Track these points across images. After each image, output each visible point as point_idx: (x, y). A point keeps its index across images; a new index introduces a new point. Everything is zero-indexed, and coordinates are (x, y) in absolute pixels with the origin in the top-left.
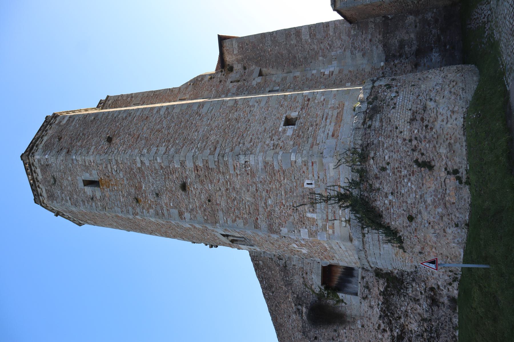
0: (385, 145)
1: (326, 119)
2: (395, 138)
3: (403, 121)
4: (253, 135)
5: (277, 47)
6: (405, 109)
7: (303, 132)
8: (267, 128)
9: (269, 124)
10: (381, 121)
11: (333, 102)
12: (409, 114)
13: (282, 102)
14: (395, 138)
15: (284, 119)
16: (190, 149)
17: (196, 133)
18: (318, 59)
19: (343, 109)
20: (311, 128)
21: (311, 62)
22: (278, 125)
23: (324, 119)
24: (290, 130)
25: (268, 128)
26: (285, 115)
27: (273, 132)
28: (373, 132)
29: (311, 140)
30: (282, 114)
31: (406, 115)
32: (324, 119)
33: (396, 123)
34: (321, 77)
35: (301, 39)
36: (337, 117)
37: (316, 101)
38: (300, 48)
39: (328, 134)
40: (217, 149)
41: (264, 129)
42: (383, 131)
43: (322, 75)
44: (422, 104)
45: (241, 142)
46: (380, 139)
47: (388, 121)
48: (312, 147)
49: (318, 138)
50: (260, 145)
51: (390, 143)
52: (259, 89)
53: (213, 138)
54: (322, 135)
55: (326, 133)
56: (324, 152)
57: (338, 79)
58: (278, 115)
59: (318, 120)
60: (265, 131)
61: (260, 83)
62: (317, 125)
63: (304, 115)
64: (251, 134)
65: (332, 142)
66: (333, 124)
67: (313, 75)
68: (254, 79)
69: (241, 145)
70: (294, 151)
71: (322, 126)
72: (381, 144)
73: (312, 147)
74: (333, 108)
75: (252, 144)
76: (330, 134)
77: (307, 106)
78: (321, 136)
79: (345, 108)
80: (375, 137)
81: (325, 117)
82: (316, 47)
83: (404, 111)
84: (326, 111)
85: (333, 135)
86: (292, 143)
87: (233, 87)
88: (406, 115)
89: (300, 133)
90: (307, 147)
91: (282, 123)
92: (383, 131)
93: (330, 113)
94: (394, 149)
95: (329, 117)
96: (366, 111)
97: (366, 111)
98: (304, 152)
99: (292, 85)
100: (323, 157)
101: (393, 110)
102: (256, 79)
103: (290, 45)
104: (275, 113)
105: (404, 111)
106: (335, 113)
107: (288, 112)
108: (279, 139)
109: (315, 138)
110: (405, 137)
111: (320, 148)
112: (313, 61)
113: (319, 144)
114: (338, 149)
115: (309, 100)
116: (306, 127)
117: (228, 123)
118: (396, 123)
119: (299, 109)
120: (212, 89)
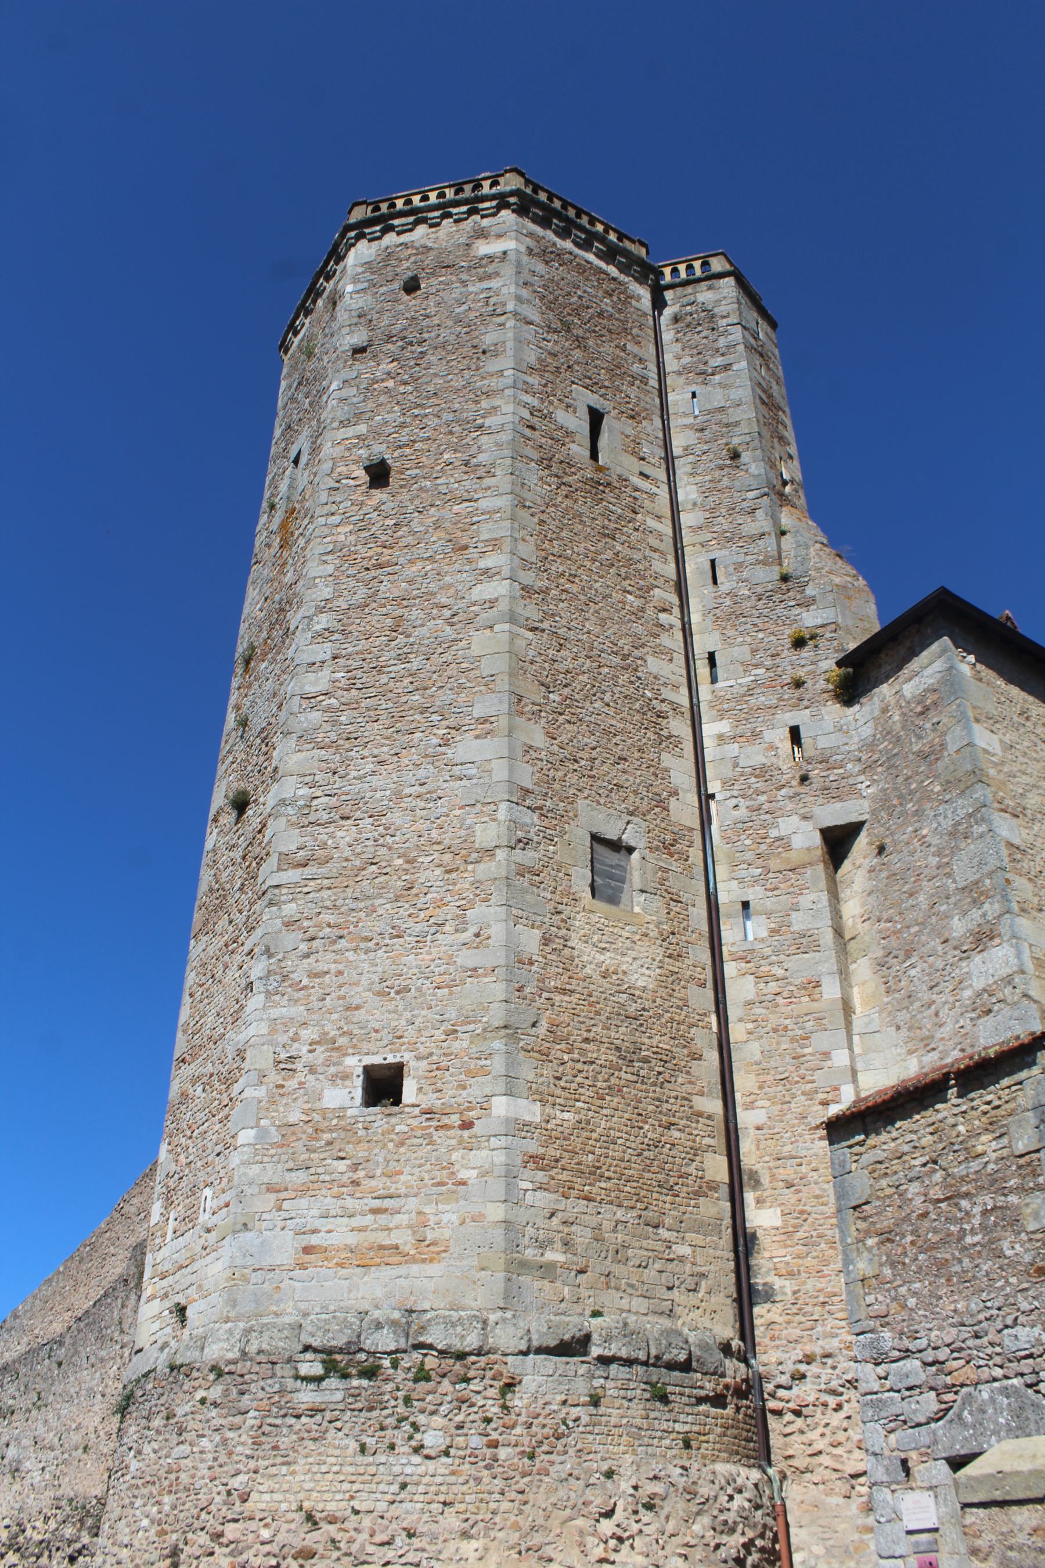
0: (231, 1435)
1: (375, 1211)
2: (252, 1464)
3: (308, 1486)
4: (340, 973)
5: (934, 861)
6: (356, 1487)
7: (329, 1143)
8: (362, 1011)
9: (376, 1014)
10: (315, 1411)
11: (445, 1218)
12: (331, 1506)
13: (471, 1027)
14: (252, 1464)
15: (391, 1059)
16: (308, 779)
17: (370, 767)
18: (910, 1052)
19: (414, 1260)
20: (342, 1166)
21: (898, 1028)
22: (365, 1046)
23: (377, 1203)
24: (346, 1096)
25: (360, 1015)
26: (407, 1057)
27: (342, 1041)
28: (277, 1387)
29: (300, 1177)
30: (413, 1046)
31: (327, 1496)
32: (377, 1203)
33: (302, 1461)
34: (809, 1095)
35: (966, 955)
36: (381, 1247)
37: (455, 1156)
38: (940, 964)
39: (314, 1232)
40: (300, 870)
41: (356, 1001)
42: (278, 1421)
43: (821, 1096)
44: (370, 1549)
45: (315, 944)
46: (252, 1414)
47: (314, 1434)
48: (271, 1189)
49: (303, 1202)
50: (298, 1011)
51: (239, 1449)
52: (759, 856)
53: (345, 834)
54: (315, 1212)
55: (318, 1223)
56: (249, 1235)
57: (804, 1169)
58: (410, 1033)
59: (373, 1183)
60: (348, 1009)
61: (788, 847)
62: (355, 1183)
63: (398, 1129)
64: (341, 967)
65: (283, 1248)
66: (352, 1239)
67: (826, 1055)
68: (805, 818)
69: (303, 947)
70: (263, 1134)
71: (350, 1202)
72: (238, 1419)
73: (271, 1189)
74: (421, 1222)
75: (305, 981)
76: (314, 1240)
77: (437, 1128)
78: (308, 1210)
79: (415, 1269)
80: (261, 1394)
81: (387, 1203)
82: (946, 1030)
83: (346, 1486)
84: (412, 1203)
85: (307, 1250)
86: (295, 1117)
87: (772, 747)
88: (326, 1496)
89: (327, 1136)
90: (272, 1173)
91: (377, 1060)
92: (278, 1421)
93: (402, 1219)
94: (221, 1466)
95: (383, 1219)
96: (361, 1350)
97: (361, 1350)
98: (256, 1169)
99: (773, 987)
100: (235, 1232)
101: (354, 1446)
102: (808, 826)
103: (947, 916)
104: (418, 1021)
105: (346, 1486)
106: (403, 1238)
107: (424, 1064)
108: (312, 1071)
109: (303, 1191)
110: (254, 1496)
111: (265, 1216)
112: (904, 1032)
113: (280, 1209)
114: (255, 1277)
115: (467, 1125)
116: (349, 1148)
117: (400, 861)
118: (302, 1461)
119: (429, 1100)
120: (756, 666)
